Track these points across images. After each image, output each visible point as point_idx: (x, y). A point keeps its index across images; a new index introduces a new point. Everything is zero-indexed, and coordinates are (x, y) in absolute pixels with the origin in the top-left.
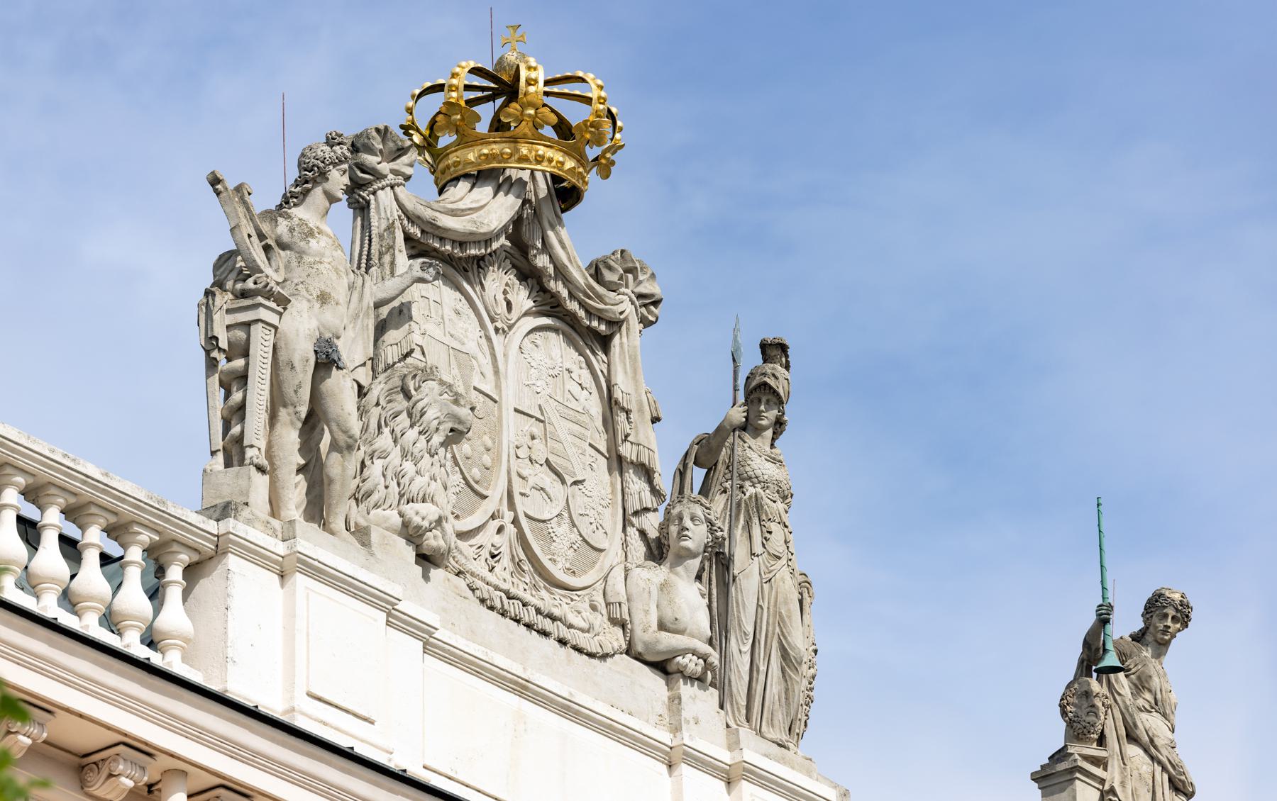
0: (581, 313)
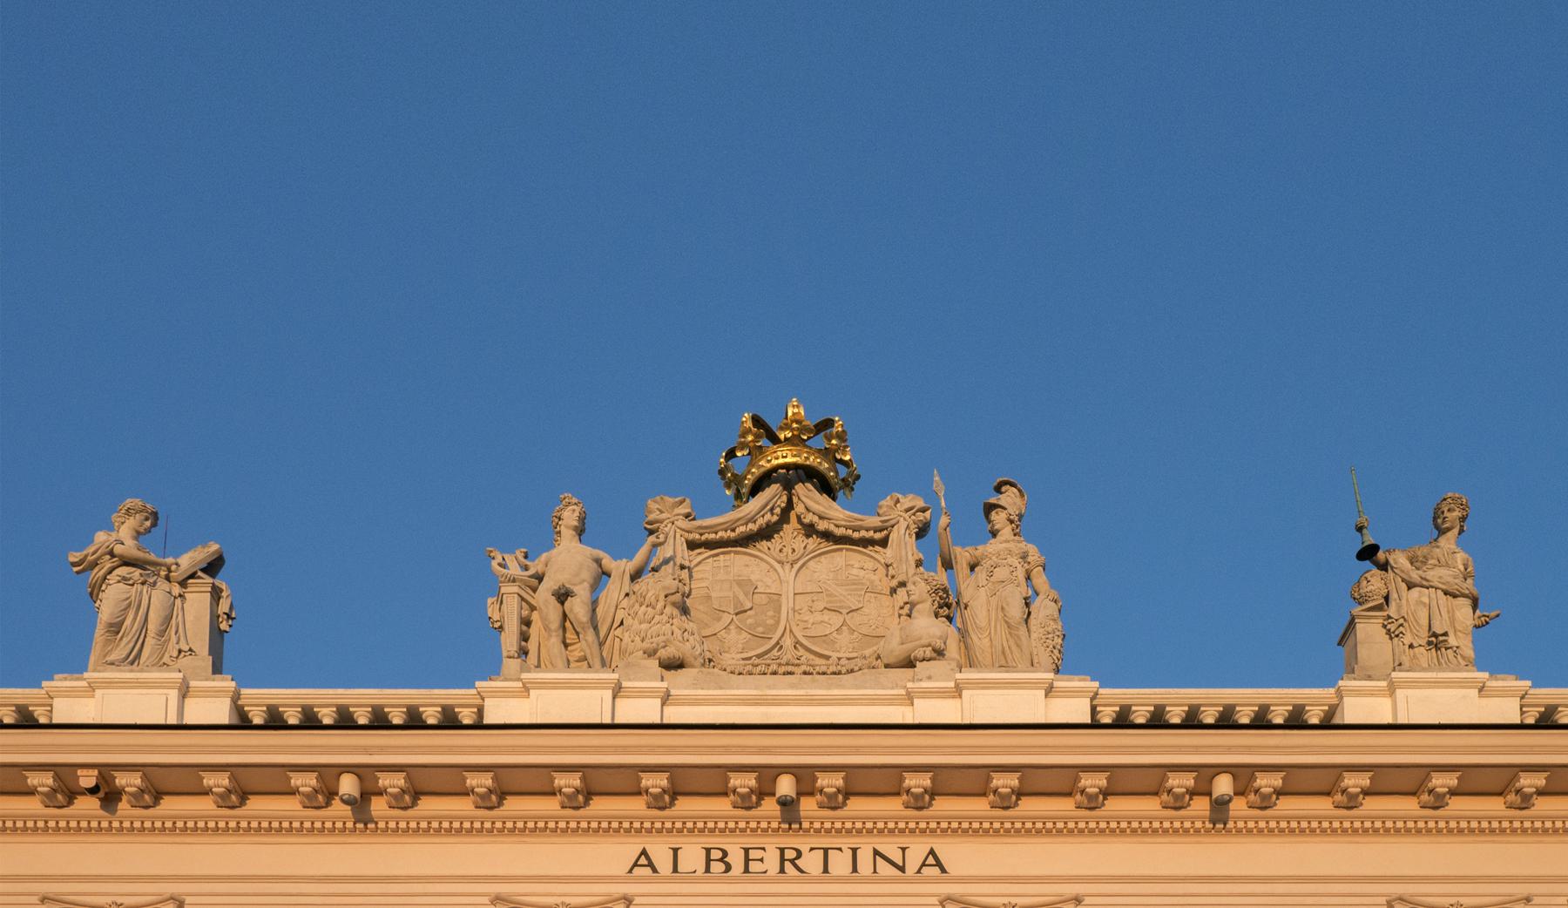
0: (850, 532)
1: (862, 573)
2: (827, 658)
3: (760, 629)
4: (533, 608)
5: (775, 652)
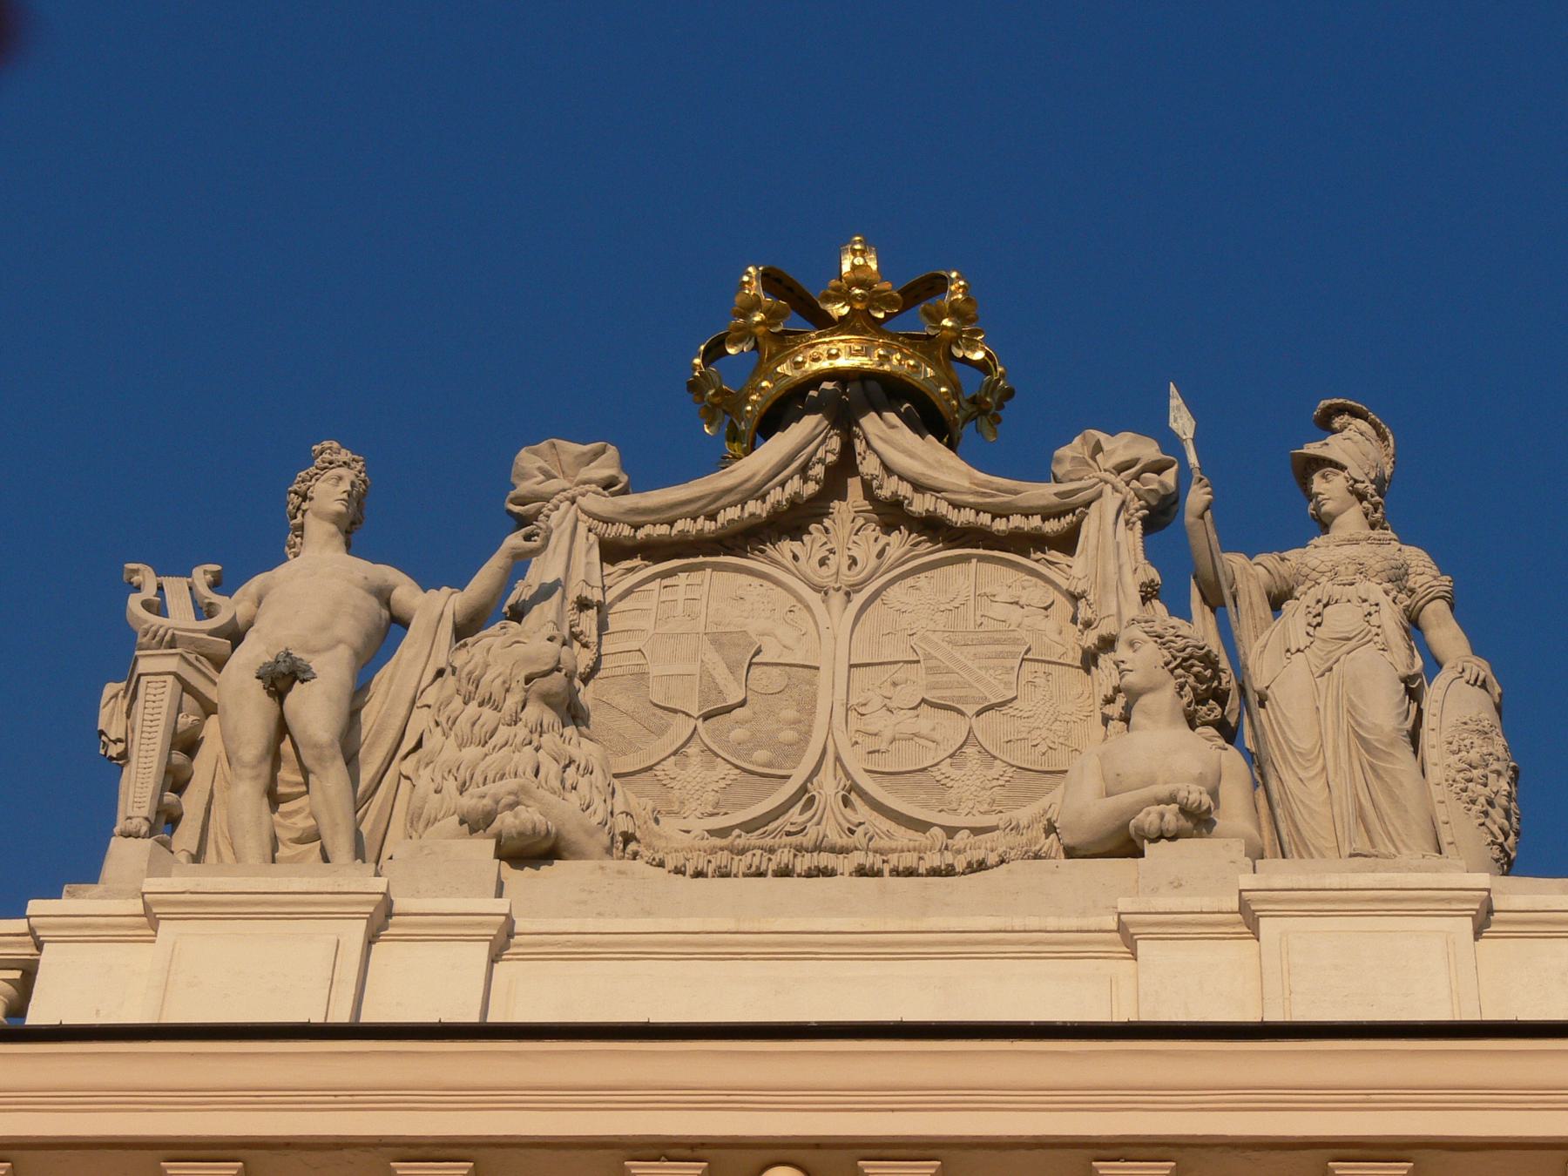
0: (985, 519)
1: (1016, 614)
2: (922, 826)
3: (761, 755)
4: (208, 708)
5: (795, 815)
